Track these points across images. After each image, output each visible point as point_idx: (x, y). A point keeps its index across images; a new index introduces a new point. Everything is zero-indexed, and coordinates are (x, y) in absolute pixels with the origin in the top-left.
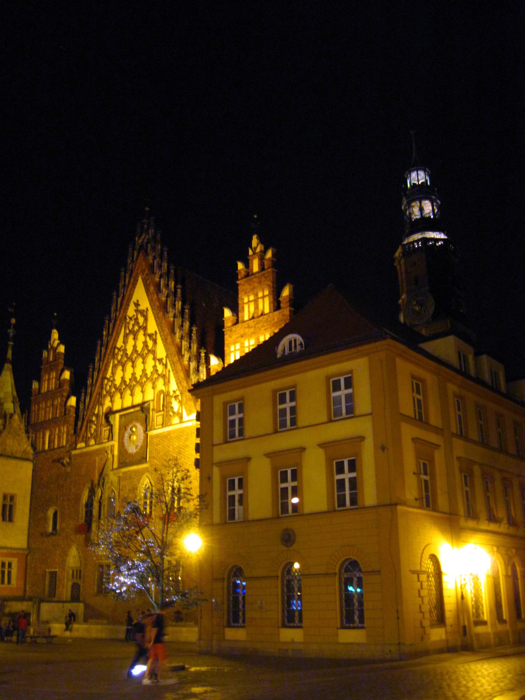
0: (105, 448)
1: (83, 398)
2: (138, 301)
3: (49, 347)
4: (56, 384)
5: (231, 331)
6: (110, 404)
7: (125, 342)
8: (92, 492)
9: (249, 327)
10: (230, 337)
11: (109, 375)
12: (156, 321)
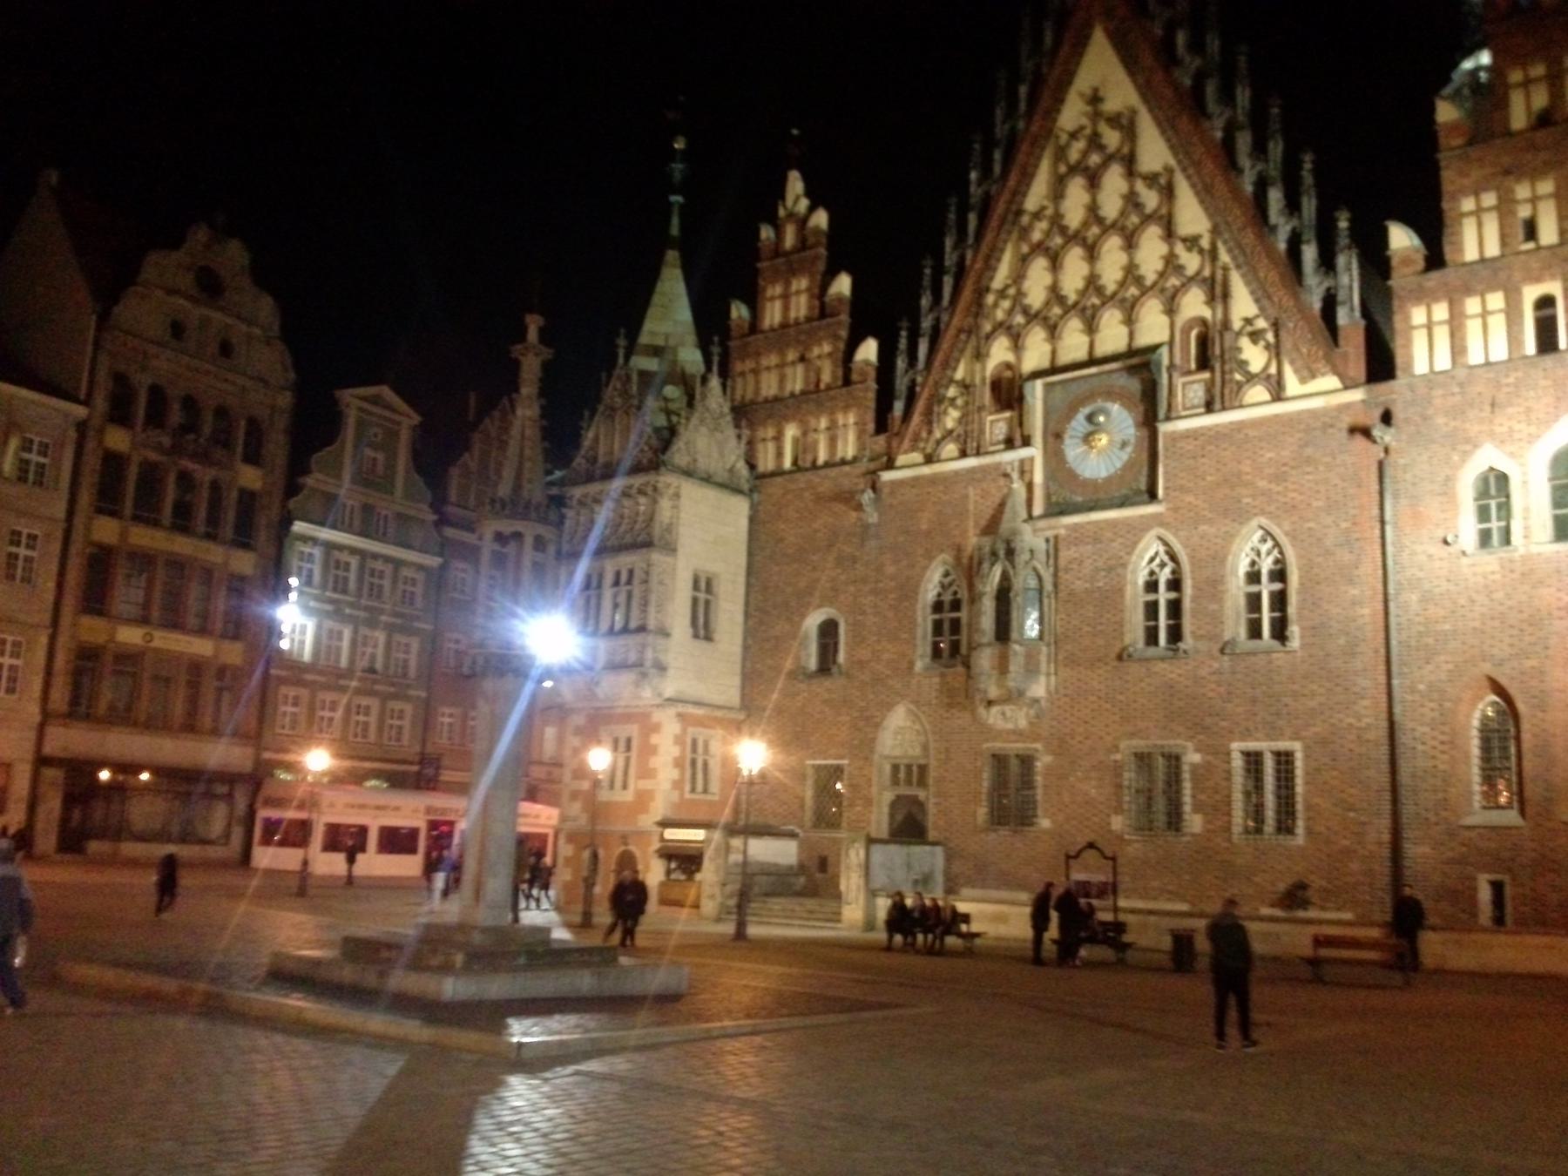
1: (903, 344)
2: (1096, 90)
3: (782, 212)
4: (810, 308)
8: (970, 570)
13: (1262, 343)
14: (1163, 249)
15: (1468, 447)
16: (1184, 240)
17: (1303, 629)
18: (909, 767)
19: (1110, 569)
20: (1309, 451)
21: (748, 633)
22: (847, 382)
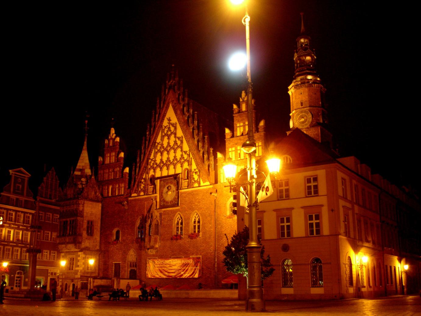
0: (151, 197)
2: (170, 118)
3: (110, 138)
4: (115, 160)
5: (230, 140)
6: (153, 174)
7: (162, 139)
8: (144, 221)
9: (240, 140)
10: (229, 144)
11: (152, 157)
12: (182, 130)
13: (197, 174)
14: (181, 153)
15: (228, 198)
16: (185, 152)
17: (202, 233)
18: (133, 263)
19: (170, 220)
20: (203, 197)
21: (101, 234)
22: (122, 177)
